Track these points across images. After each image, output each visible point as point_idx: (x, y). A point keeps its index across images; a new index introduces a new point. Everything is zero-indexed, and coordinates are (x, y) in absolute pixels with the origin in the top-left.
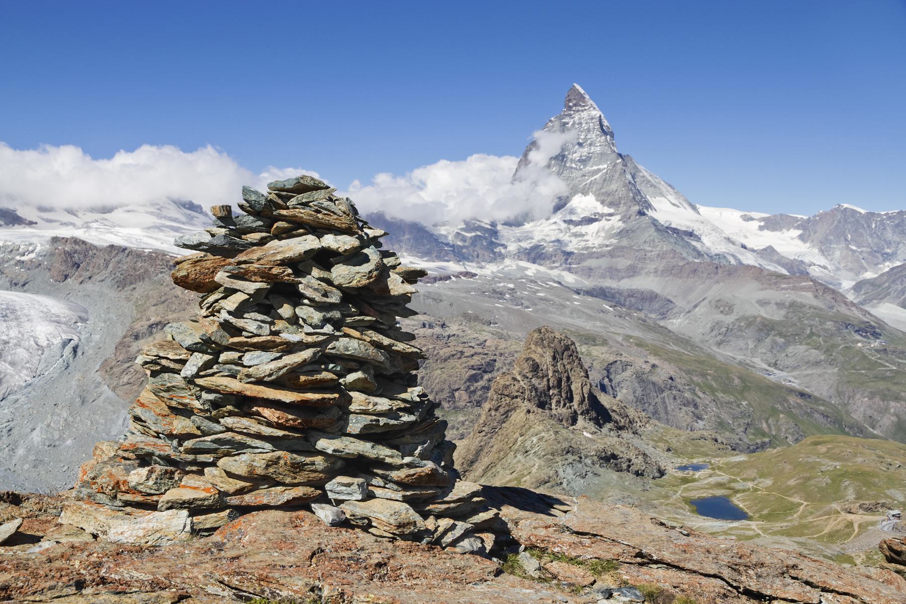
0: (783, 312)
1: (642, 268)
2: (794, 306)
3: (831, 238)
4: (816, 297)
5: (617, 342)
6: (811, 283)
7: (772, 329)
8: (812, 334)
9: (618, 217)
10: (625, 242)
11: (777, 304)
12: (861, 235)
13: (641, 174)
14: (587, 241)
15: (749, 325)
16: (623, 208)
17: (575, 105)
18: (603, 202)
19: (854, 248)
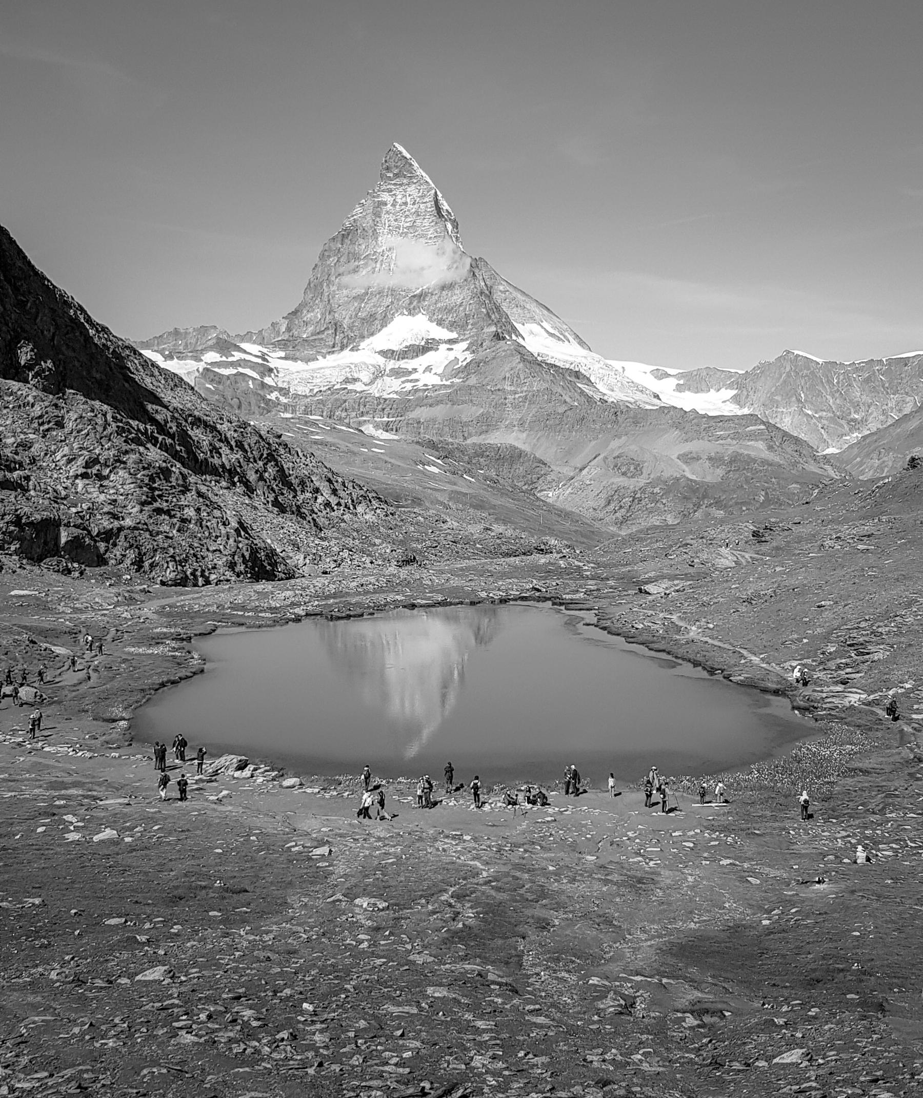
0: (720, 472)
1: (501, 420)
2: (737, 462)
3: (778, 398)
4: (770, 448)
5: (441, 503)
6: (763, 427)
7: (704, 497)
8: (768, 500)
9: (464, 345)
10: (473, 380)
11: (710, 459)
12: (820, 394)
13: (501, 288)
14: (417, 380)
15: (667, 492)
16: (470, 331)
17: (397, 176)
18: (440, 323)
19: (810, 412)
